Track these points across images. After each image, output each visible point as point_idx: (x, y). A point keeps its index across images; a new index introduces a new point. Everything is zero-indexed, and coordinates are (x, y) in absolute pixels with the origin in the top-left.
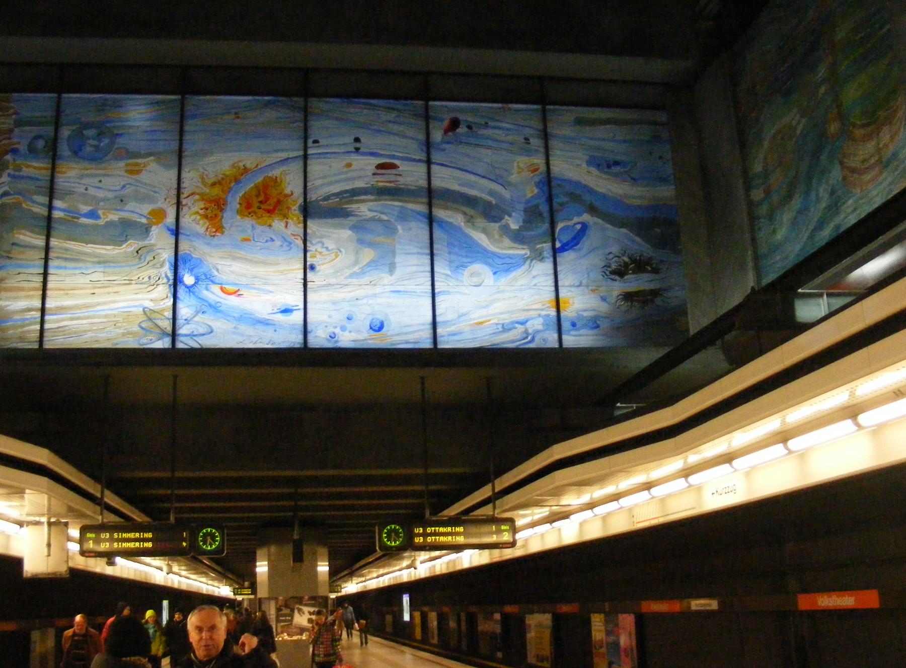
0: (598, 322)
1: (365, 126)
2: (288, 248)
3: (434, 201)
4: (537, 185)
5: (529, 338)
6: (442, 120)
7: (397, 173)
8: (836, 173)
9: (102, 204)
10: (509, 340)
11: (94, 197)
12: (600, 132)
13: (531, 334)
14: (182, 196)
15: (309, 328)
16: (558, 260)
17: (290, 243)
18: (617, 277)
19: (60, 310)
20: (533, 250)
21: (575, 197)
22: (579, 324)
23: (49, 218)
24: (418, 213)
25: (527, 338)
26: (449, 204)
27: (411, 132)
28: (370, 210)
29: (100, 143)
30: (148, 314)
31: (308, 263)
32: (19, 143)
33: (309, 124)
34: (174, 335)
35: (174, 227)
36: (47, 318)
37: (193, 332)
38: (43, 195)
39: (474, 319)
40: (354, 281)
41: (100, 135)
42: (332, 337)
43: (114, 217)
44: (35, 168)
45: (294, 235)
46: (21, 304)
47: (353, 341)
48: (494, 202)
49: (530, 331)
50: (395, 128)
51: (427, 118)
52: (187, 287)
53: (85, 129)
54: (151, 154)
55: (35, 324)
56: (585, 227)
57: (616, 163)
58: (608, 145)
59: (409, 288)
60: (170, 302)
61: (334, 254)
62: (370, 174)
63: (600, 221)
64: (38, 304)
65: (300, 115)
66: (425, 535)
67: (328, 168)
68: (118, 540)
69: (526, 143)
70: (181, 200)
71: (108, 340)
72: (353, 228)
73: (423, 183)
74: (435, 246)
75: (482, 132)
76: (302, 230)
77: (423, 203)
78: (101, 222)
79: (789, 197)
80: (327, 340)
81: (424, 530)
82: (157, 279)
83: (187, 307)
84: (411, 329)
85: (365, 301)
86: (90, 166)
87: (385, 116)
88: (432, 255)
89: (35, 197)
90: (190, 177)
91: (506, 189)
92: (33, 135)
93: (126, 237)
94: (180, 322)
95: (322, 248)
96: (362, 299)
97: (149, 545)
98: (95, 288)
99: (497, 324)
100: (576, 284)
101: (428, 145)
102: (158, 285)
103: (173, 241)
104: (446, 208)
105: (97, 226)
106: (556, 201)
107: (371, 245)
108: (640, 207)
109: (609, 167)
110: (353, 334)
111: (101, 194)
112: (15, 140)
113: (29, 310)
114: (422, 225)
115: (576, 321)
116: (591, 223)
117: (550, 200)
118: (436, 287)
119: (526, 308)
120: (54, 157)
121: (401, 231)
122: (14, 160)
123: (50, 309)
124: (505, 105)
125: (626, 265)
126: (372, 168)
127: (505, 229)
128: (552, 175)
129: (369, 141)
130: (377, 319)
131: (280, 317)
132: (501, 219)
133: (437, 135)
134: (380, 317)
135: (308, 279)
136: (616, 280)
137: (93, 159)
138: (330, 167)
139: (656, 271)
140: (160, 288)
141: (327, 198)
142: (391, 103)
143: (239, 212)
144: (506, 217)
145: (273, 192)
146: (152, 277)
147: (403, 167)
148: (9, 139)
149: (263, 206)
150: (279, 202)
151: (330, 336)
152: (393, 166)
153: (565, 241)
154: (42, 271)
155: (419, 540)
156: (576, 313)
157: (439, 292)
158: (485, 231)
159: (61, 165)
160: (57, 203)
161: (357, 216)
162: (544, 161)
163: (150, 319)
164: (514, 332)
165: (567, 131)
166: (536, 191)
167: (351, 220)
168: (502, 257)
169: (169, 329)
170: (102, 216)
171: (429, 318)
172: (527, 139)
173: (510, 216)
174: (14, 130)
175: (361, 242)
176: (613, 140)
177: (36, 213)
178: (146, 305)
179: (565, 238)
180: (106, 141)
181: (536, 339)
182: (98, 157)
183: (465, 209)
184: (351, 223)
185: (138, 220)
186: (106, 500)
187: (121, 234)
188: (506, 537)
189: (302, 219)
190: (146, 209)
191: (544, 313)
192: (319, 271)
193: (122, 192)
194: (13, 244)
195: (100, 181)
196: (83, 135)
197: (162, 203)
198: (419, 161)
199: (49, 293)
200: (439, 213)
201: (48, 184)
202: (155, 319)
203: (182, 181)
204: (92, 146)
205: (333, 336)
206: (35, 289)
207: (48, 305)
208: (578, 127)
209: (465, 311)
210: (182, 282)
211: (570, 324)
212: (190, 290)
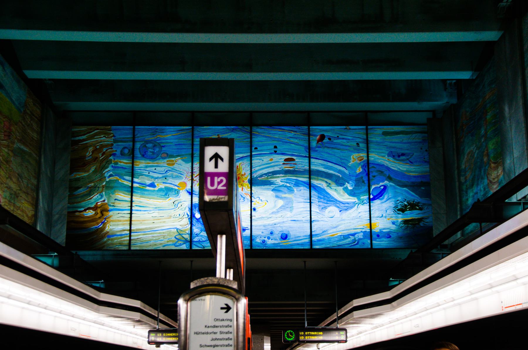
0: (391, 235)
1: (279, 140)
2: (244, 200)
3: (312, 177)
4: (362, 167)
5: (356, 242)
6: (316, 136)
7: (294, 163)
8: (486, 181)
9: (156, 180)
10: (346, 243)
11: (152, 177)
12: (396, 139)
13: (357, 240)
14: (194, 176)
15: (253, 238)
16: (371, 204)
17: (244, 198)
18: (401, 212)
19: (138, 231)
20: (359, 199)
21: (381, 172)
22: (381, 235)
23: (132, 187)
24: (304, 182)
25: (355, 242)
26: (319, 178)
27: (301, 143)
28: (281, 181)
29: (155, 151)
30: (179, 232)
31: (252, 208)
32: (116, 151)
33: (253, 139)
34: (191, 242)
35: (190, 191)
36: (132, 234)
37: (200, 240)
38: (129, 176)
39: (330, 233)
40: (274, 215)
41: (154, 146)
42: (264, 242)
43: (163, 186)
44: (124, 163)
45: (246, 194)
46: (120, 227)
47: (273, 244)
48: (341, 176)
49: (357, 239)
51: (309, 135)
53: (147, 144)
54: (178, 156)
55: (127, 237)
56: (385, 187)
57: (403, 155)
59: (299, 219)
61: (264, 203)
62: (281, 163)
63: (393, 184)
64: (128, 227)
65: (248, 135)
66: (304, 335)
67: (262, 161)
68: (165, 337)
69: (358, 146)
70: (193, 178)
71: (161, 244)
72: (273, 190)
73: (307, 167)
74: (312, 198)
75: (335, 141)
76: (250, 192)
77: (307, 178)
78: (156, 189)
79: (472, 185)
80: (261, 243)
81: (304, 333)
82: (183, 215)
83: (197, 228)
84: (300, 238)
85: (279, 225)
86: (150, 162)
88: (310, 203)
89: (125, 177)
91: (347, 170)
92: (122, 147)
93: (168, 196)
94: (194, 235)
95: (259, 200)
96: (277, 224)
98: (154, 220)
99: (341, 236)
100: (380, 216)
101: (309, 149)
102: (183, 218)
103: (190, 197)
104: (318, 180)
105: (154, 191)
106: (371, 176)
107: (281, 198)
108: (414, 177)
109: (399, 156)
110: (273, 240)
111: (156, 175)
112: (114, 149)
113: (124, 230)
114: (305, 188)
115: (379, 234)
116: (389, 185)
117: (368, 175)
118: (312, 218)
119: (355, 228)
121: (296, 191)
122: (114, 159)
123: (134, 230)
124: (347, 127)
127: (346, 189)
128: (370, 162)
130: (284, 233)
132: (344, 185)
134: (286, 233)
135: (253, 215)
136: (400, 214)
137: (152, 158)
138: (263, 161)
139: (420, 209)
140: (185, 219)
141: (261, 176)
144: (347, 183)
146: (180, 215)
148: (112, 149)
151: (263, 242)
153: (375, 194)
154: (129, 212)
155: (302, 338)
156: (380, 230)
157: (314, 221)
160: (135, 180)
161: (275, 184)
162: (366, 155)
163: (180, 234)
164: (349, 239)
165: (378, 139)
166: (361, 170)
168: (344, 203)
169: (189, 239)
170: (157, 186)
171: (309, 233)
173: (348, 183)
174: (113, 144)
175: (277, 197)
176: (401, 143)
177: (126, 185)
178: (178, 228)
181: (360, 243)
183: (326, 180)
184: (273, 188)
185: (173, 188)
186: (160, 318)
187: (166, 194)
188: (343, 338)
189: (249, 186)
190: (177, 182)
191: (364, 230)
192: (257, 211)
193: (165, 174)
194: (115, 200)
195: (155, 169)
196: (146, 147)
197: (185, 180)
198: (306, 157)
199: (133, 222)
200: (314, 182)
201: (131, 171)
202: (182, 234)
203: (194, 169)
204: (151, 152)
205: (264, 241)
206: (127, 221)
207: (132, 228)
208: (384, 137)
209: (325, 229)
210: (194, 216)
211: (376, 236)
212: (198, 221)
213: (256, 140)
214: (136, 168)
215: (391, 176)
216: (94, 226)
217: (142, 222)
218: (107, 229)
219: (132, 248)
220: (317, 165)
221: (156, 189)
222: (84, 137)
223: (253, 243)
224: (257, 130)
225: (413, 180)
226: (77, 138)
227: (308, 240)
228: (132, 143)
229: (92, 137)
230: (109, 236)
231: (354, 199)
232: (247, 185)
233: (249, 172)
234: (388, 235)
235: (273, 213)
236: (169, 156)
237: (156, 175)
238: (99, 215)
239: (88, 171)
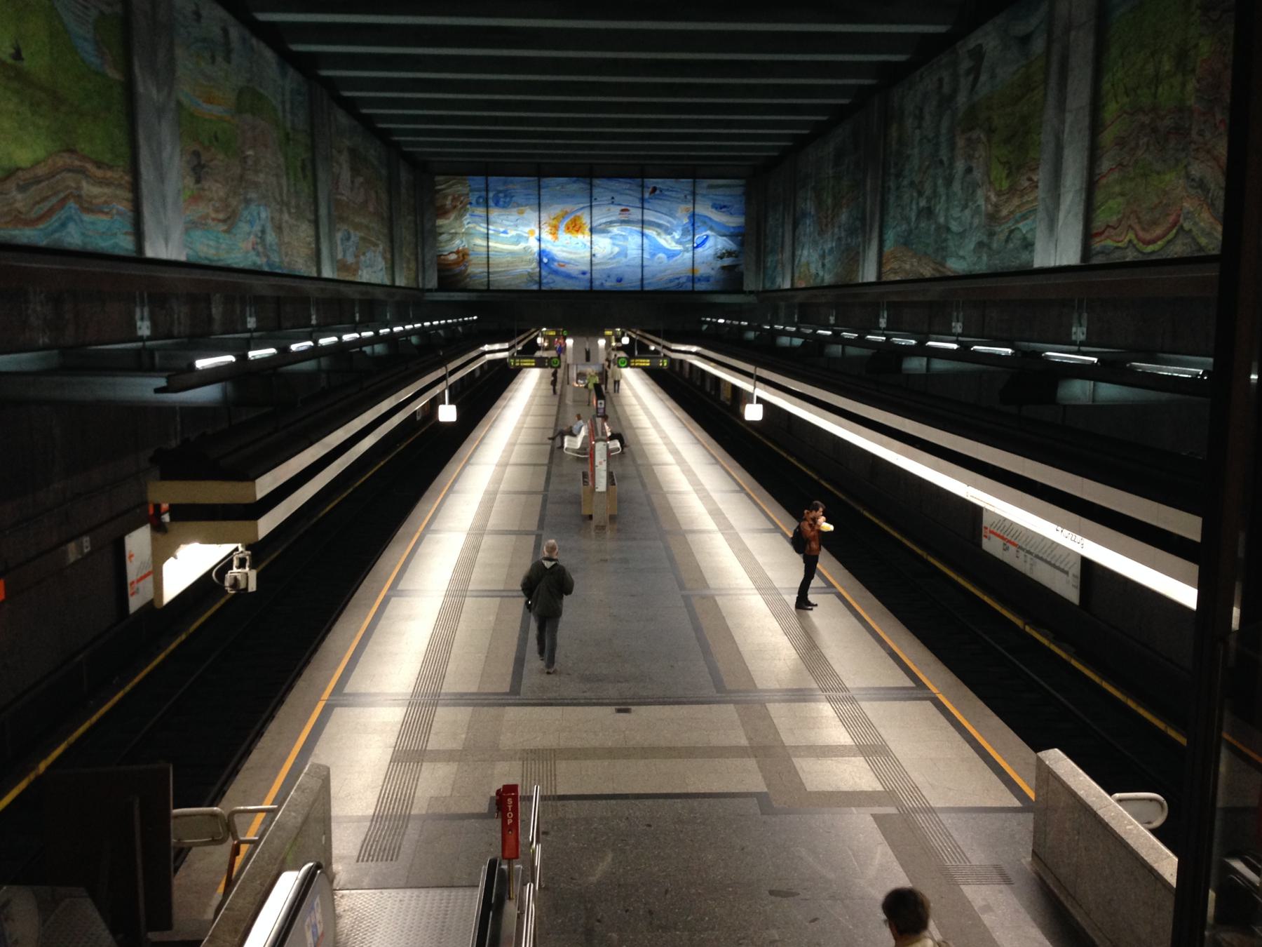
1: (616, 191)
10: (672, 286)
20: (684, 247)
21: (705, 223)
23: (488, 234)
41: (505, 196)
42: (602, 284)
46: (480, 270)
50: (628, 192)
51: (642, 186)
52: (546, 264)
58: (721, 198)
60: (538, 270)
64: (486, 270)
65: (589, 187)
72: (611, 238)
73: (640, 217)
75: (666, 193)
78: (508, 236)
87: (625, 186)
90: (543, 215)
97: (533, 364)
101: (643, 200)
104: (649, 229)
106: (696, 225)
107: (617, 245)
108: (733, 227)
109: (721, 208)
113: (483, 272)
117: (693, 225)
120: (487, 207)
125: (724, 254)
126: (618, 212)
129: (618, 198)
131: (582, 276)
137: (504, 207)
139: (736, 257)
141: (600, 225)
142: (629, 181)
143: (565, 231)
145: (578, 222)
147: (632, 210)
149: (575, 228)
150: (580, 227)
158: (665, 239)
159: (490, 209)
160: (491, 227)
165: (704, 192)
167: (609, 235)
171: (640, 276)
172: (686, 196)
175: (614, 244)
176: (724, 195)
179: (699, 242)
180: (508, 200)
190: (527, 229)
200: (647, 231)
213: (595, 191)
214: (490, 216)
215: (713, 225)
216: (457, 269)
217: (498, 265)
219: (491, 288)
220: (649, 216)
221: (508, 236)
222: (443, 187)
223: (593, 284)
224: (596, 182)
225: (732, 230)
226: (439, 187)
227: (639, 283)
228: (484, 193)
229: (451, 186)
230: (471, 277)
231: (679, 248)
232: (587, 232)
233: (589, 221)
234: (707, 279)
235: (610, 259)
236: (519, 205)
237: (507, 223)
238: (461, 258)
239: (449, 218)
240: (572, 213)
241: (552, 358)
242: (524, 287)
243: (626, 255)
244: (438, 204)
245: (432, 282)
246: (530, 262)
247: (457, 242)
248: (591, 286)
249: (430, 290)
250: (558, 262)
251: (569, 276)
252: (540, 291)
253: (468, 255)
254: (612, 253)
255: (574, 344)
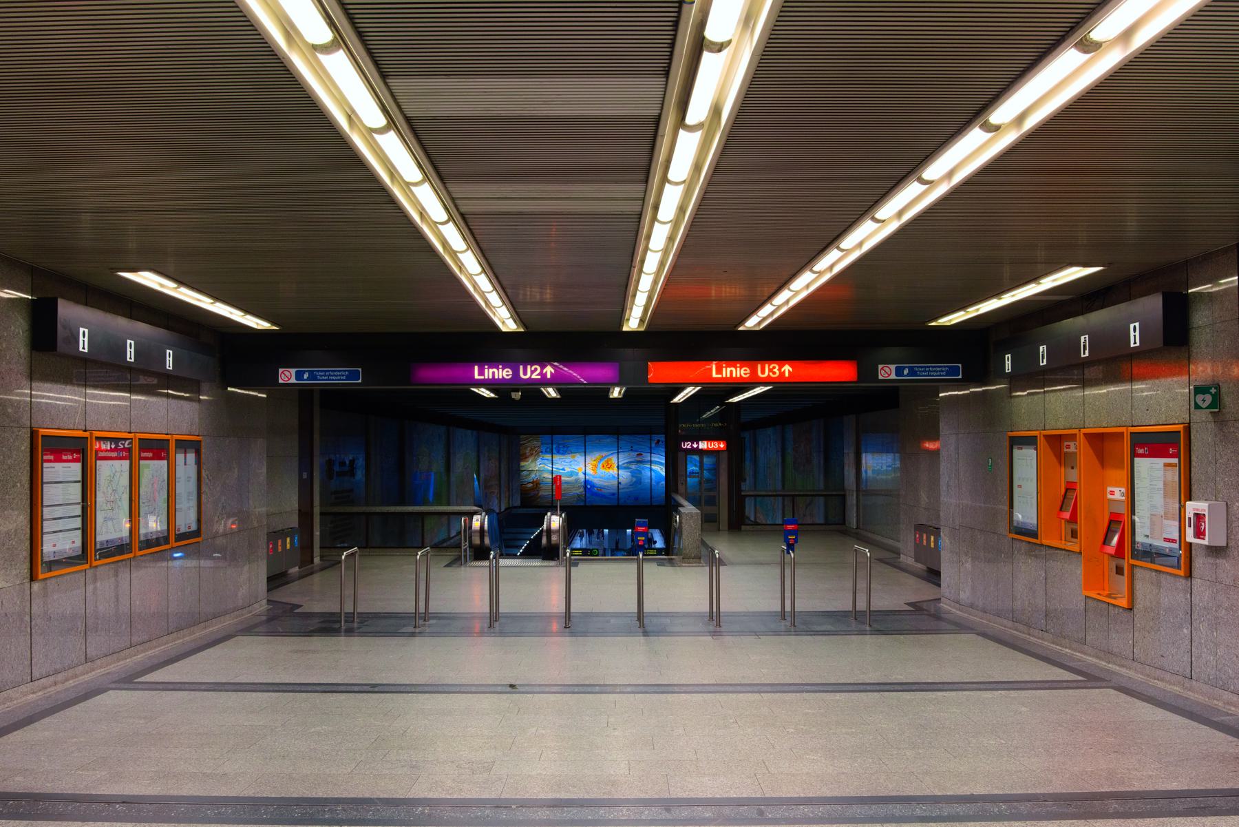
34: (585, 501)
43: (569, 470)
60: (584, 493)
73: (649, 459)
108: (710, 465)
129: (635, 447)
133: (653, 445)
141: (624, 464)
152: (642, 455)
160: (554, 466)
175: (632, 476)
180: (565, 449)
182: (564, 453)
190: (577, 467)
200: (653, 467)
216: (532, 493)
218: (540, 493)
224: (621, 437)
229: (529, 442)
235: (631, 485)
240: (606, 456)
241: (593, 549)
242: (575, 504)
243: (641, 483)
244: (521, 452)
245: (518, 503)
246: (579, 487)
247: (533, 476)
248: (618, 503)
249: (516, 507)
250: (597, 487)
251: (603, 496)
252: (585, 506)
253: (540, 484)
254: (632, 481)
255: (609, 532)
